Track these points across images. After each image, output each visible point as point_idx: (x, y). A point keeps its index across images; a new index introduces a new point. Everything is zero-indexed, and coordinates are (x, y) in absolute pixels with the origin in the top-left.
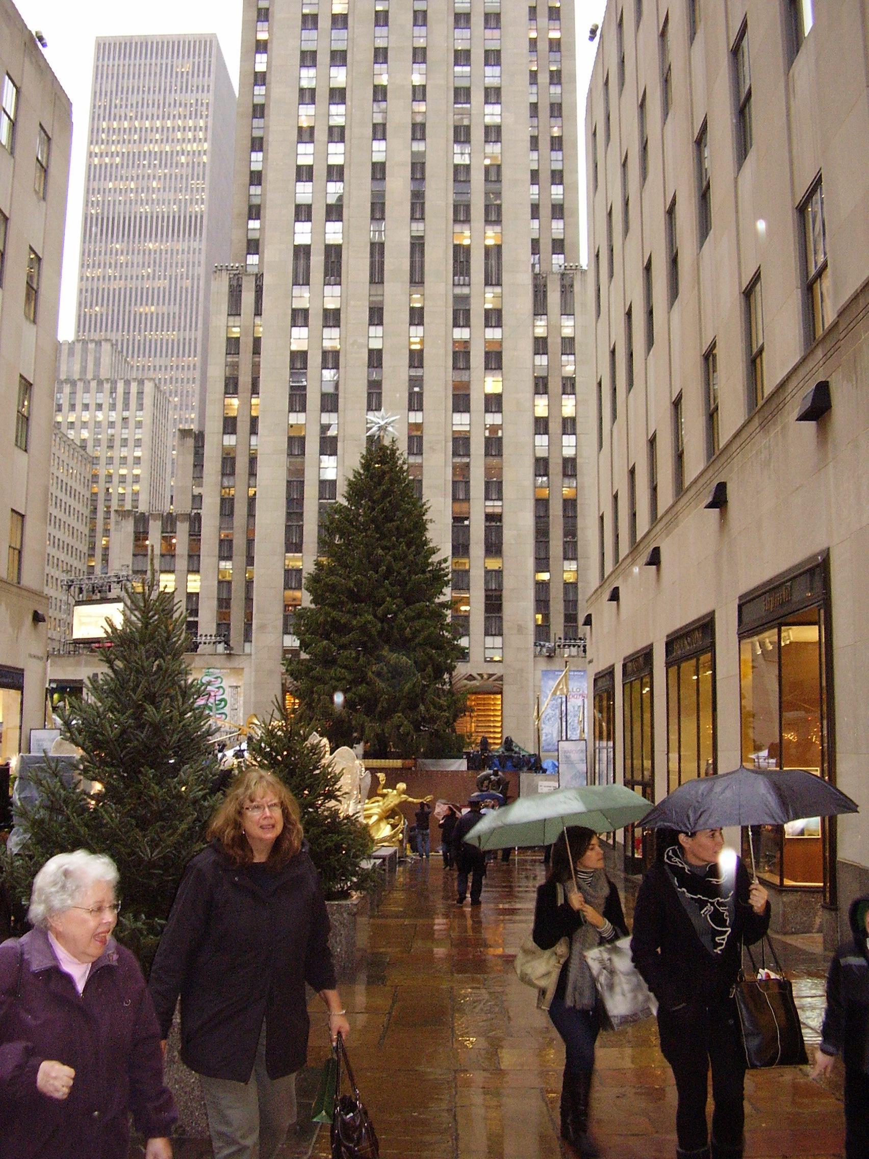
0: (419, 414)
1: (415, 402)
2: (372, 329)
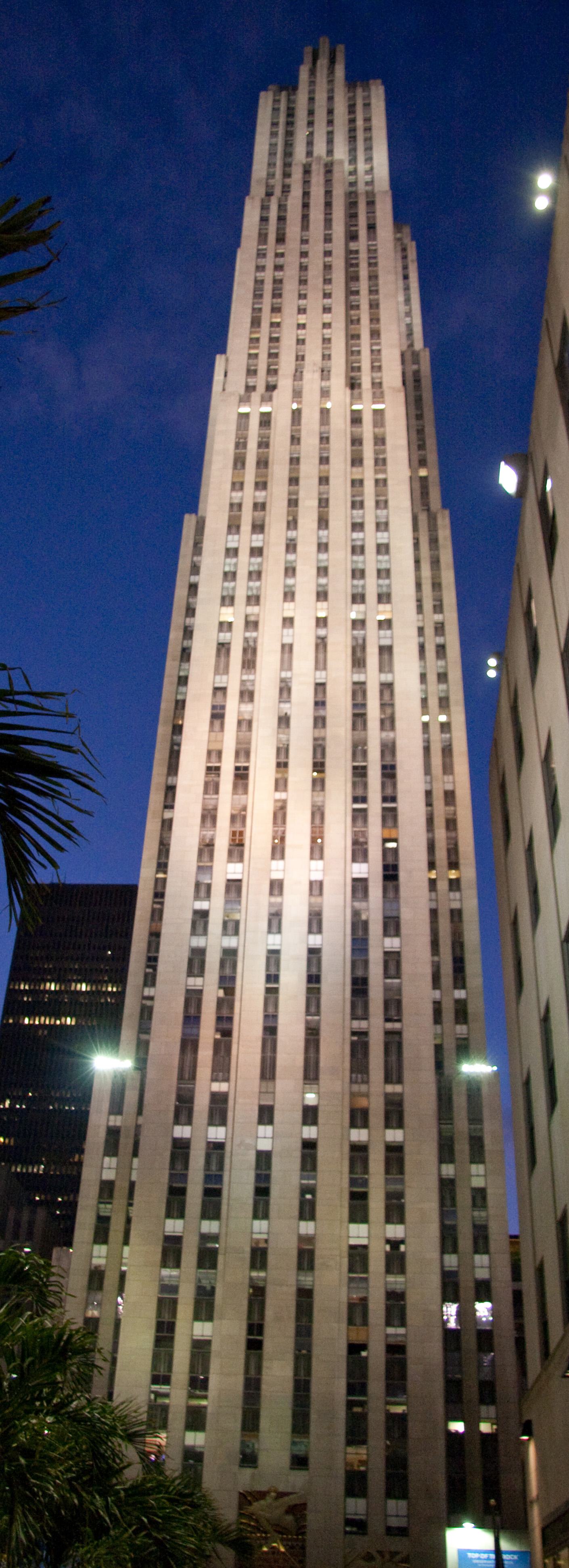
0: (311, 1224)
1: (307, 1211)
2: (261, 1128)
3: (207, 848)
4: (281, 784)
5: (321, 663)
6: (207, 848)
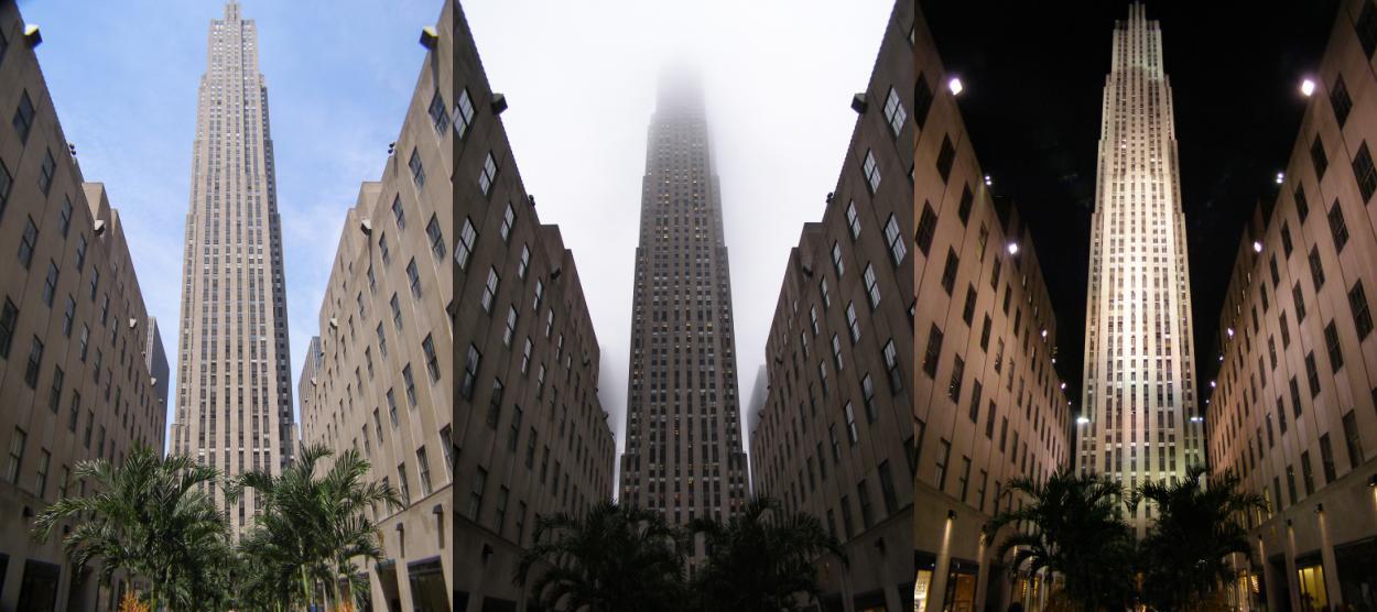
3: (1110, 352)
4: (1133, 329)
5: (1144, 285)
6: (1110, 352)
